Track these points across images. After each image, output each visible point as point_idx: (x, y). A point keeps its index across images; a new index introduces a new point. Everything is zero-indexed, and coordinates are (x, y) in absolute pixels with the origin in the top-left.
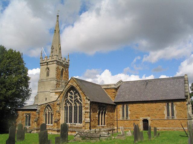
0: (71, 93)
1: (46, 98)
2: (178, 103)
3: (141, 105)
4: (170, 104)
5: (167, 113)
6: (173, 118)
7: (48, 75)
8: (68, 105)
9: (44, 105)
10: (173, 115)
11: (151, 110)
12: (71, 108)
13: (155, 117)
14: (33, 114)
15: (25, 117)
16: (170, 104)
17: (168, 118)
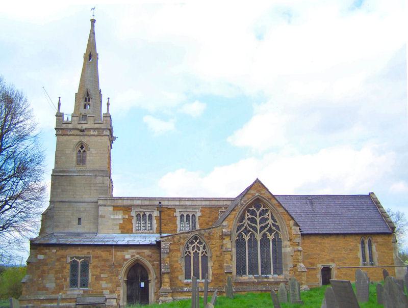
0: (253, 213)
1: (80, 219)
2: (380, 239)
3: (318, 240)
4: (367, 241)
5: (363, 256)
6: (372, 265)
7: (81, 160)
8: (247, 238)
9: (182, 235)
10: (371, 259)
11: (337, 250)
12: (253, 242)
13: (344, 263)
14: (97, 257)
15: (69, 266)
16: (367, 241)
17: (365, 265)
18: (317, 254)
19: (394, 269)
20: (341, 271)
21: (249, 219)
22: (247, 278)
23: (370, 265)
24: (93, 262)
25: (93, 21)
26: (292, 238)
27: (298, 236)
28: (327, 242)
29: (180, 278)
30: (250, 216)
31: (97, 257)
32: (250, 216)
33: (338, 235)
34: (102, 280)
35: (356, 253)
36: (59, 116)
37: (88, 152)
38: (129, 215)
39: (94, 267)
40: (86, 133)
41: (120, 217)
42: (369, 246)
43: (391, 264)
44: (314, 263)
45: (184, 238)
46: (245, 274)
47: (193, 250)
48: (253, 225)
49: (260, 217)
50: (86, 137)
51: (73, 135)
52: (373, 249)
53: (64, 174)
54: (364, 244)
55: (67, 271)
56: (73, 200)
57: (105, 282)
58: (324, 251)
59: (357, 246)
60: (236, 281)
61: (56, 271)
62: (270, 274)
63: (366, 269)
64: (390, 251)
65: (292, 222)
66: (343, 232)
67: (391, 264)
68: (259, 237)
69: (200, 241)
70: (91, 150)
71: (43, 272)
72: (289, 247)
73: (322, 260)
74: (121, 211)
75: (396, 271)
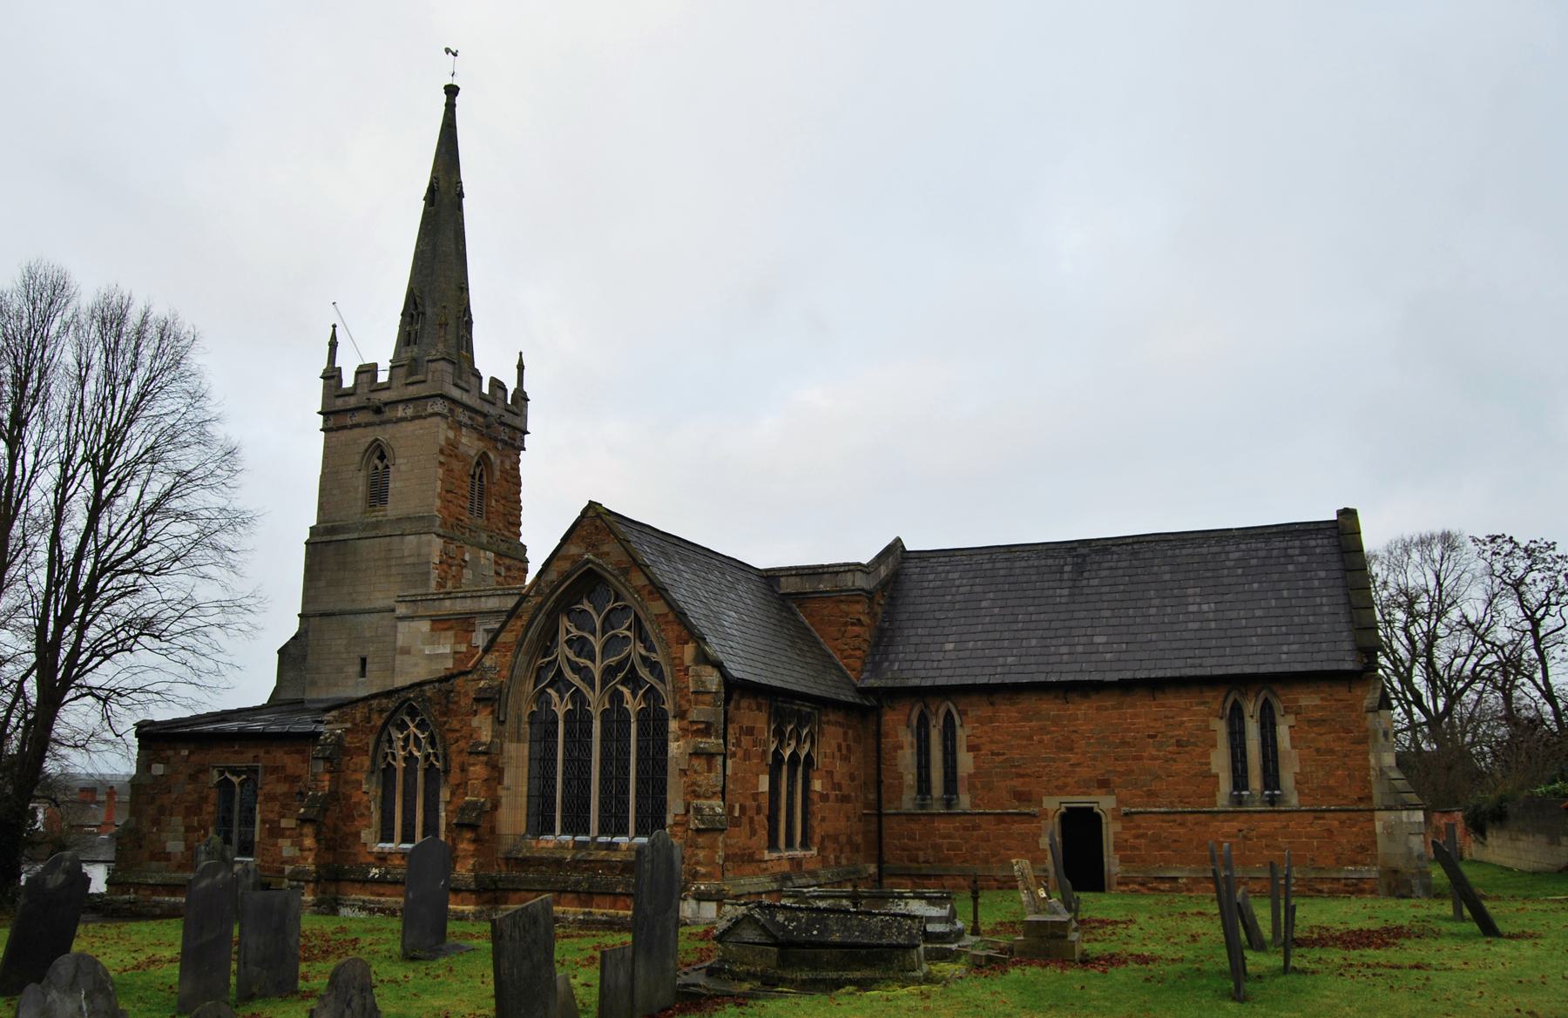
0: (582, 620)
1: (364, 661)
2: (1308, 699)
3: (1050, 707)
4: (1251, 708)
5: (1234, 770)
6: (1272, 803)
7: (378, 493)
8: (561, 708)
9: (375, 703)
10: (1271, 777)
11: (1124, 743)
12: (578, 722)
13: (1151, 794)
14: (274, 770)
15: (214, 795)
16: (1251, 708)
17: (1240, 803)
18: (1044, 760)
19: (1372, 820)
20: (1139, 827)
21: (569, 642)
22: (558, 840)
23: (1263, 803)
24: (271, 785)
25: (452, 91)
26: (686, 706)
27: (708, 698)
28: (1082, 711)
29: (365, 835)
30: (575, 632)
31: (274, 770)
32: (575, 632)
33: (1127, 687)
34: (283, 836)
35: (1206, 755)
36: (331, 375)
37: (392, 469)
38: (470, 644)
39: (271, 798)
40: (388, 414)
41: (447, 650)
42: (1263, 727)
43: (1361, 799)
44: (1030, 793)
45: (381, 711)
46: (552, 832)
47: (404, 748)
48: (582, 661)
49: (604, 632)
50: (388, 426)
51: (357, 426)
52: (1279, 739)
53: (335, 538)
54: (1242, 719)
55: (211, 809)
56: (348, 606)
57: (288, 842)
58: (1071, 750)
59: (1207, 729)
60: (514, 854)
61: (187, 808)
62: (625, 833)
63: (1245, 816)
64: (1360, 748)
65: (689, 651)
66: (983, 680)
67: (1361, 799)
68: (597, 702)
69: (423, 720)
70: (398, 461)
71: (162, 810)
72: (677, 740)
73: (1060, 783)
74: (450, 633)
75: (1379, 826)
